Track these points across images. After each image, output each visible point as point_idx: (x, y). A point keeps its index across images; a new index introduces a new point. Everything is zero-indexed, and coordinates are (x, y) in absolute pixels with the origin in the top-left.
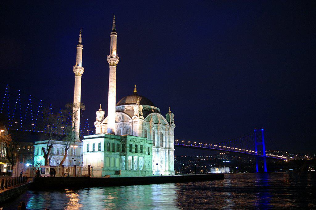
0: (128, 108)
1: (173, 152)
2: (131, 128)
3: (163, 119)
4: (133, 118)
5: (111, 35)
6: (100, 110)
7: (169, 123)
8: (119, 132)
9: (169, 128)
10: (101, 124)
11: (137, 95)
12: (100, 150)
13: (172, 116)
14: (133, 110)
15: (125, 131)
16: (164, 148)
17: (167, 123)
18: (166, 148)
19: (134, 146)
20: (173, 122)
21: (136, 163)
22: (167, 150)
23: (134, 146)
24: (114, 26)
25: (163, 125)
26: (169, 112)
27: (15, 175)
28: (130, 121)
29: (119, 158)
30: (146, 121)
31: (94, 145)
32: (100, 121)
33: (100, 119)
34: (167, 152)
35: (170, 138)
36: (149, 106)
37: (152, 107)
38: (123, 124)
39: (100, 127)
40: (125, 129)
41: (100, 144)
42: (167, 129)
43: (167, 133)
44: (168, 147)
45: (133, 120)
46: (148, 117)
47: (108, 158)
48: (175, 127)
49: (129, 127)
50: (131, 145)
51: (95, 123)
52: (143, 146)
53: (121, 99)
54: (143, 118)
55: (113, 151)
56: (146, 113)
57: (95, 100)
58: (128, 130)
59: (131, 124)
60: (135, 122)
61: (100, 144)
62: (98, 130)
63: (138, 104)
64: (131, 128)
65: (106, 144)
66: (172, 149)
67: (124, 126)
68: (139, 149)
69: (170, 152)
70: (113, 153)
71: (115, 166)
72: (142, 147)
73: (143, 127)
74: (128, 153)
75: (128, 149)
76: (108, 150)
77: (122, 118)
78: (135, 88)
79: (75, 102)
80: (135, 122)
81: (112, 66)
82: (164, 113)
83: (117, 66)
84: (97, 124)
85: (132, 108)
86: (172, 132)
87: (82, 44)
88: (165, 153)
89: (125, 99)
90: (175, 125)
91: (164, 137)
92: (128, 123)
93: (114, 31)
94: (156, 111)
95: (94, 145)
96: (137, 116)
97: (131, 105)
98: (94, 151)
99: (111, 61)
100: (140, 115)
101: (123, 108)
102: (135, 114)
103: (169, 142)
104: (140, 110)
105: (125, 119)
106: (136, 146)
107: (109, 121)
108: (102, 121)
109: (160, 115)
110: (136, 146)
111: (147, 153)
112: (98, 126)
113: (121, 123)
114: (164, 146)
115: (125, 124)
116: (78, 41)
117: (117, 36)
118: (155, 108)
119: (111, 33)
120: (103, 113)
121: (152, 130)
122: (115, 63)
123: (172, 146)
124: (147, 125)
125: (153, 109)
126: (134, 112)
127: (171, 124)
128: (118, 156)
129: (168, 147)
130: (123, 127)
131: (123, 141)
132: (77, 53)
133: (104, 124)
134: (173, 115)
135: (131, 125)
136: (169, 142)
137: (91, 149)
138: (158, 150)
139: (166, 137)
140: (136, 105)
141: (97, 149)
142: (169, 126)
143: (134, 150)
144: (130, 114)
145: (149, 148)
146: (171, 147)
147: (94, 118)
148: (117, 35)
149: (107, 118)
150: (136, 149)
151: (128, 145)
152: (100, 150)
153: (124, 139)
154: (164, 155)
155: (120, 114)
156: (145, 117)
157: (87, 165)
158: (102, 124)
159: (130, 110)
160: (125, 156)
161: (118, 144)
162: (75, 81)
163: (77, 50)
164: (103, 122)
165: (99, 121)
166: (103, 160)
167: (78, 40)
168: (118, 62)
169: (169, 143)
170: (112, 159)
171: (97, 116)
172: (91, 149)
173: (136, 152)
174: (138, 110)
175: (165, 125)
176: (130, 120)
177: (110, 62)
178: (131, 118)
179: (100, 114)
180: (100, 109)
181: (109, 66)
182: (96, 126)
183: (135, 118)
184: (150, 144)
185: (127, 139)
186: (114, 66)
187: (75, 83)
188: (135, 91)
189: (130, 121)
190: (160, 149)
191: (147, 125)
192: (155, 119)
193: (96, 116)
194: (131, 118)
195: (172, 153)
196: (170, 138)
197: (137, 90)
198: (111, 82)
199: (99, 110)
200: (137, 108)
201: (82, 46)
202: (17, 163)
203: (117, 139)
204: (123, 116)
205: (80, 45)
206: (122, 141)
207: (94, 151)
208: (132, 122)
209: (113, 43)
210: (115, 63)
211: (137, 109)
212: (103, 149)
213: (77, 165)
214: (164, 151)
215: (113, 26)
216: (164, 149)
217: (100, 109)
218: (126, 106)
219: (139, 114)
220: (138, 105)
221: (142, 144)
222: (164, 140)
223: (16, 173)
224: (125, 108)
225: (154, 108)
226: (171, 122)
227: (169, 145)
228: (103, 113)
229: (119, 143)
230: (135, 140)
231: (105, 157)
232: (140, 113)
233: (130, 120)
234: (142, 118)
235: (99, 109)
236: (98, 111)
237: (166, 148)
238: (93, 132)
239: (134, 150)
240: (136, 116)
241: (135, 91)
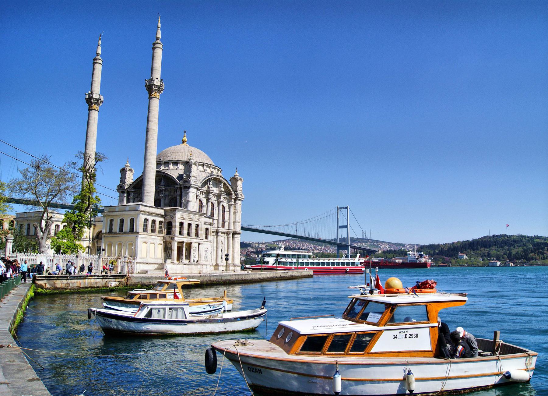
19: (186, 226)
23: (186, 226)
28: (176, 186)
50: (181, 224)
52: (200, 226)
72: (197, 226)
75: (177, 230)
106: (189, 225)
110: (189, 225)
111: (204, 236)
114: (226, 226)
137: (116, 228)
143: (185, 232)
145: (207, 229)
150: (189, 230)
151: (177, 224)
172: (116, 228)
189: (176, 186)
229: (162, 220)
239: (185, 232)
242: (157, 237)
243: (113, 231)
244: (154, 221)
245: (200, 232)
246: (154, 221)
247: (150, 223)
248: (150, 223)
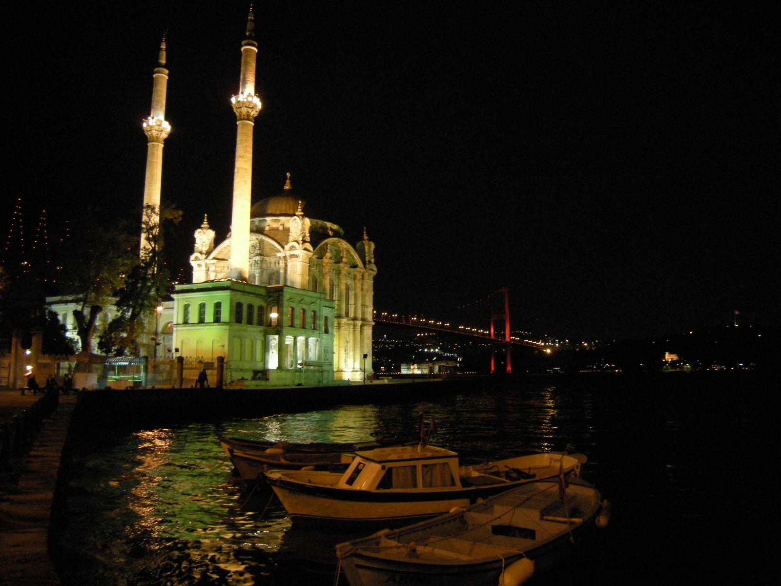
0: (275, 225)
1: (371, 328)
2: (282, 271)
3: (352, 253)
4: (287, 247)
5: (242, 46)
6: (205, 228)
7: (364, 263)
8: (252, 276)
9: (363, 276)
10: (207, 261)
11: (294, 194)
12: (217, 320)
13: (370, 247)
14: (287, 231)
15: (265, 277)
16: (352, 320)
17: (359, 263)
18: (355, 319)
20: (373, 260)
21: (283, 356)
22: (359, 323)
24: (250, 26)
25: (351, 267)
26: (363, 239)
27: (6, 380)
28: (279, 255)
29: (263, 339)
30: (316, 256)
31: (202, 307)
32: (205, 252)
33: (205, 249)
34: (358, 328)
35: (363, 297)
36: (320, 222)
37: (329, 224)
38: (262, 261)
39: (204, 268)
40: (265, 273)
41: (218, 306)
42: (359, 276)
43: (359, 285)
44: (359, 316)
45: (288, 253)
46: (321, 247)
47: (237, 341)
48: (375, 273)
49: (275, 269)
51: (192, 257)
53: (262, 196)
54: (311, 249)
55: (250, 322)
56: (316, 237)
57: (201, 200)
58: (274, 275)
59: (281, 262)
60: (292, 256)
61: (218, 306)
62: (199, 276)
63: (301, 215)
64: (282, 271)
65: (234, 304)
66: (369, 321)
67: (264, 266)
68: (309, 320)
69: (365, 328)
70: (250, 328)
71: (253, 358)
73: (309, 270)
74: (285, 330)
76: (238, 320)
77: (260, 247)
78: (288, 181)
79: (146, 201)
80: (292, 256)
81: (244, 119)
82: (353, 239)
83: (254, 123)
84: (197, 259)
85: (283, 225)
86: (369, 283)
87: (166, 66)
88: (354, 331)
89: (266, 204)
90: (375, 268)
91: (351, 293)
92: (272, 259)
93: (250, 37)
94: (336, 234)
95: (202, 307)
96: (297, 241)
97: (282, 219)
98: (186, 323)
99: (242, 109)
100: (304, 241)
101: (263, 225)
102: (291, 238)
103: (363, 305)
104: (303, 229)
105: (267, 249)
107: (229, 254)
108: (208, 253)
109: (344, 245)
112: (199, 265)
113: (258, 258)
114: (352, 315)
115: (266, 261)
116: (158, 60)
117: (256, 50)
118: (335, 227)
119: (243, 42)
120: (211, 234)
121: (328, 278)
122: (252, 114)
123: (369, 317)
124: (317, 265)
125: (331, 229)
126: (290, 234)
127: (367, 266)
128: (260, 338)
129: (359, 316)
130: (261, 268)
131: (272, 299)
132: (154, 89)
133: (215, 261)
134: (373, 246)
135: (282, 264)
136: (362, 305)
137: (194, 317)
138: (339, 324)
139: (355, 295)
140: (296, 217)
141: (209, 316)
142: (363, 270)
143: (298, 322)
144: (282, 237)
146: (366, 317)
147: (189, 246)
148: (257, 48)
149: (226, 243)
152: (217, 320)
153: (276, 295)
154: (351, 335)
155: (255, 237)
156: (314, 243)
157: (216, 356)
158: (209, 261)
159: (277, 229)
160: (277, 337)
161: (256, 304)
162: (149, 153)
163: (155, 81)
164: (213, 255)
165: (201, 253)
166: (226, 343)
167: (157, 57)
168: (257, 113)
169: (362, 309)
170: (247, 342)
171: (197, 241)
173: (303, 327)
174: (300, 228)
175: (355, 266)
176: (280, 252)
177: (239, 110)
178: (283, 248)
179: (204, 237)
180: (205, 224)
181: (236, 120)
182: (193, 263)
183: (292, 248)
184: (330, 309)
185: (282, 295)
186: (248, 122)
187: (149, 159)
188: (287, 187)
189: (279, 255)
190: (344, 321)
191: (317, 265)
192: (334, 253)
193: (193, 241)
194: (283, 248)
195: (368, 331)
196: (363, 297)
197: (291, 183)
198: (240, 159)
199: (201, 228)
200: (296, 226)
201: (167, 71)
202: (13, 351)
203: (258, 295)
204: (261, 242)
205: (161, 69)
206: (269, 300)
207: (201, 321)
208: (285, 257)
209: (247, 65)
210: (252, 114)
211: (298, 225)
212: (225, 315)
213: (149, 356)
214: (352, 327)
215: (248, 25)
216: (352, 322)
217: (205, 224)
218: (268, 219)
219: (301, 239)
220: (301, 217)
221: (313, 307)
222: (352, 301)
223: (12, 376)
224: (267, 223)
225: (332, 227)
226: (367, 262)
227: (363, 313)
228: (211, 234)
230: (300, 299)
231: (232, 337)
232: (304, 237)
233: (280, 252)
234: (308, 248)
235: (202, 226)
236: (199, 230)
237: (355, 319)
238: (187, 276)
239: (298, 322)
240: (295, 244)
241: (287, 187)
242: (255, 329)
243: (190, 321)
244: (250, 307)
245: (318, 322)
246: (250, 307)
247: (245, 308)
248: (245, 308)
